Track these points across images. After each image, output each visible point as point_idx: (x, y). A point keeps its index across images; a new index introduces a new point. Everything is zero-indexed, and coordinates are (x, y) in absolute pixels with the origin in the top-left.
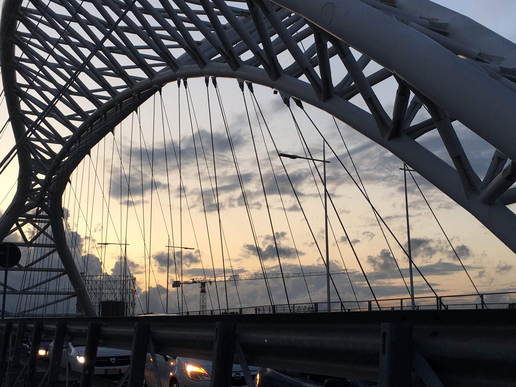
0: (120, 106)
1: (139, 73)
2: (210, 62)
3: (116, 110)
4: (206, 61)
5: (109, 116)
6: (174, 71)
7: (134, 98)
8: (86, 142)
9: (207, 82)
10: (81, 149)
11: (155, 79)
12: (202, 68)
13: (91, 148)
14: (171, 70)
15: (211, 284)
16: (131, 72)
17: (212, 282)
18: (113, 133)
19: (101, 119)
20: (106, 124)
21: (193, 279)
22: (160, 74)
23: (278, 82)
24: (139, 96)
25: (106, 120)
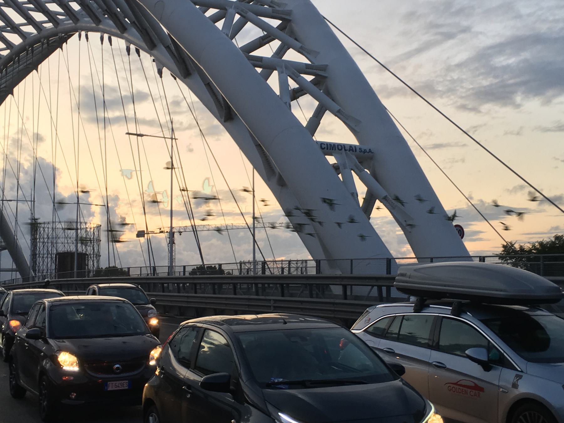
0: (32, 51)
1: (29, 29)
2: (106, 19)
3: (27, 54)
4: (101, 18)
5: (35, 50)
6: (76, 23)
7: (43, 44)
8: (6, 82)
9: (102, 39)
10: (3, 88)
11: (60, 28)
12: (97, 25)
13: (14, 88)
14: (71, 21)
15: (180, 234)
16: (24, 29)
17: (182, 232)
18: (37, 71)
19: (14, 62)
20: (28, 62)
21: (160, 229)
22: (65, 22)
23: (154, 52)
24: (48, 43)
25: (20, 63)
